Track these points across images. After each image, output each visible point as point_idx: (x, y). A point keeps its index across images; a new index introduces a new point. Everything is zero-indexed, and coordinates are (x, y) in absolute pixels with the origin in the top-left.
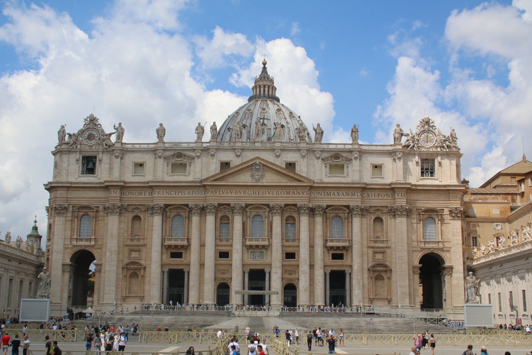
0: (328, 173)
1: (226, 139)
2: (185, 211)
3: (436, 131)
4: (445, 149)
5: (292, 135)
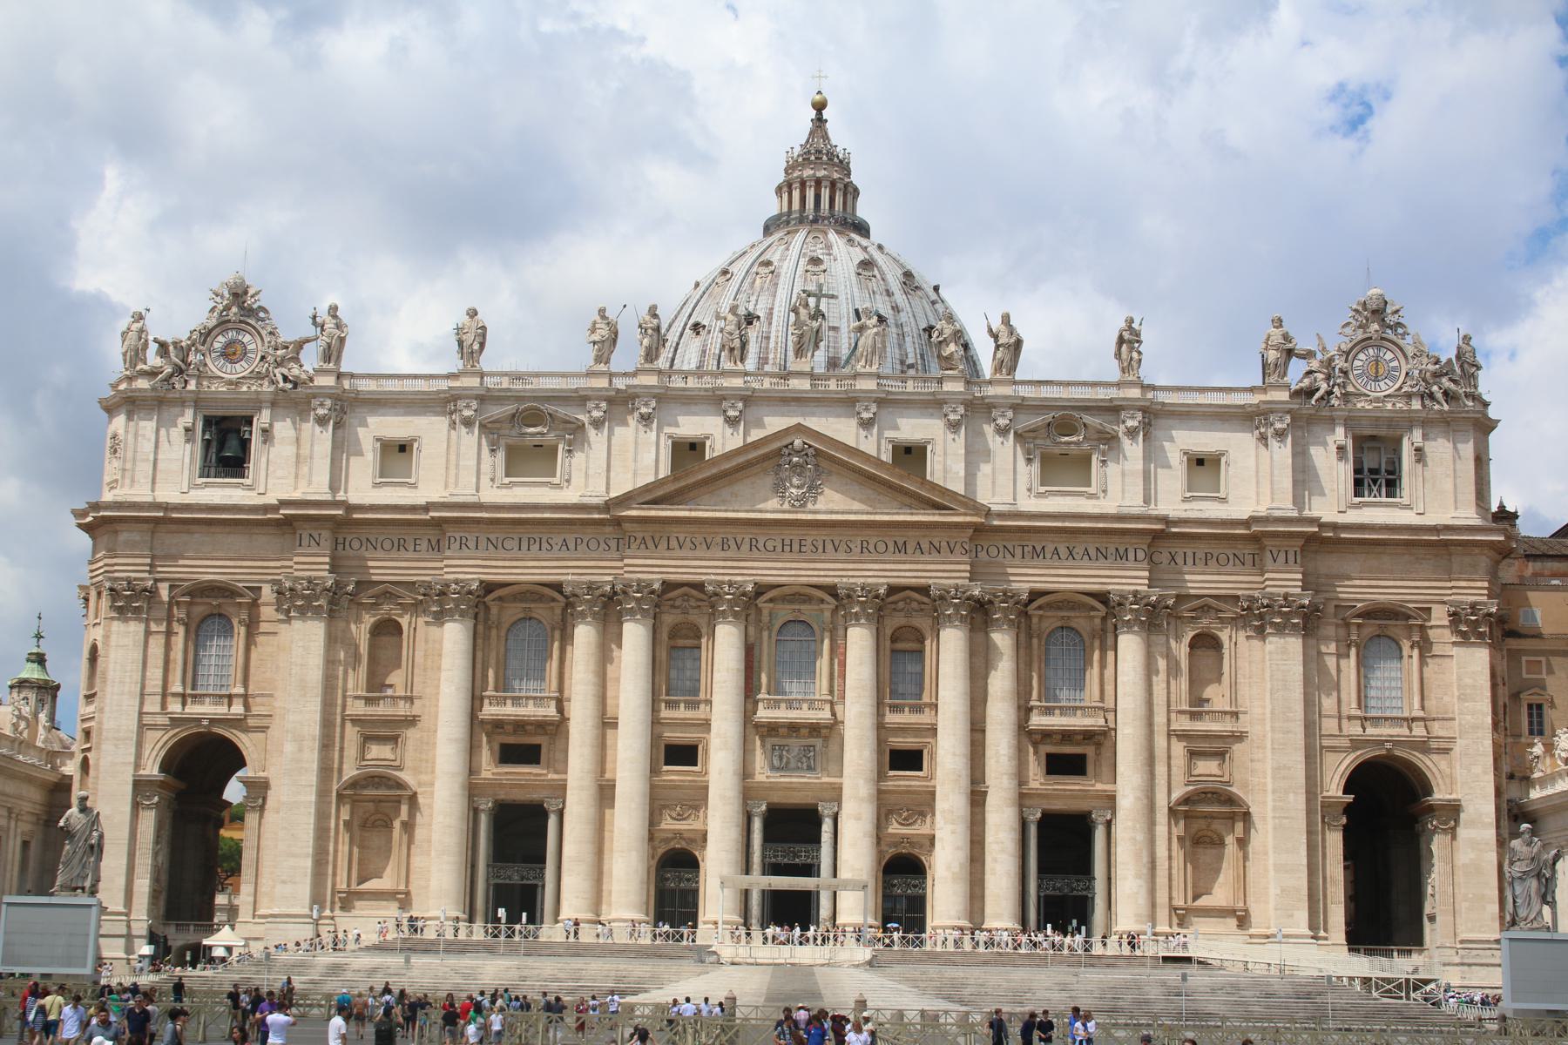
0: (1035, 485)
1: (686, 362)
2: (552, 604)
3: (1408, 344)
4: (1439, 403)
5: (910, 350)
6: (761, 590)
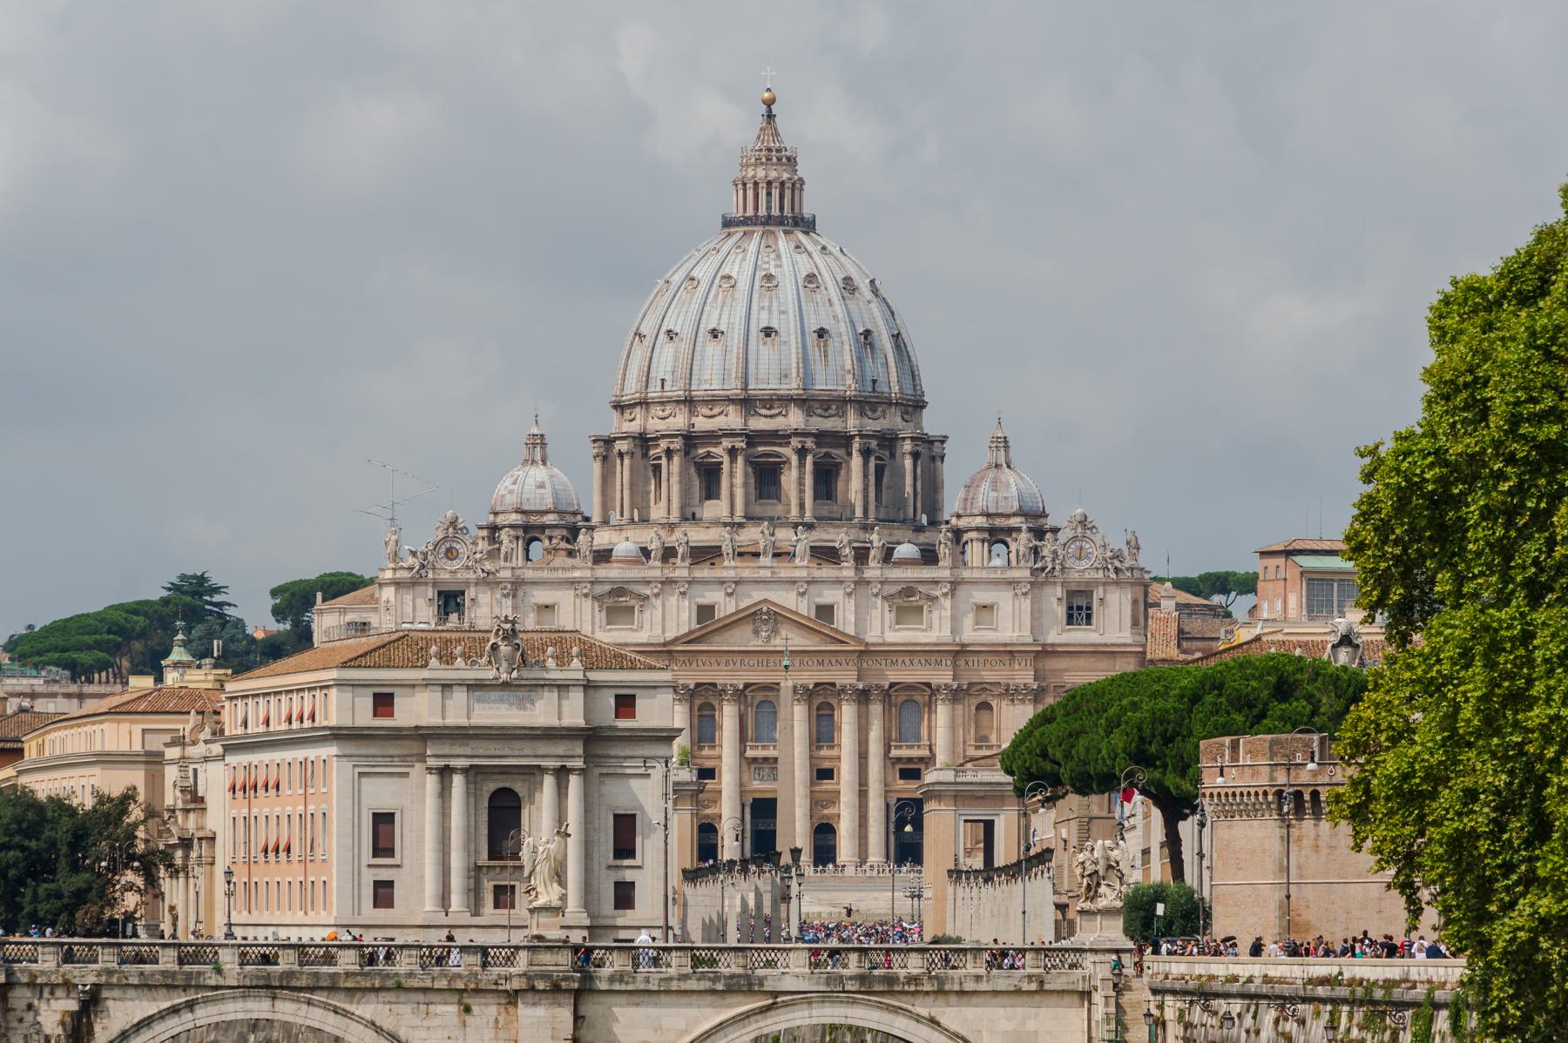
3: (1098, 539)
6: (747, 686)
